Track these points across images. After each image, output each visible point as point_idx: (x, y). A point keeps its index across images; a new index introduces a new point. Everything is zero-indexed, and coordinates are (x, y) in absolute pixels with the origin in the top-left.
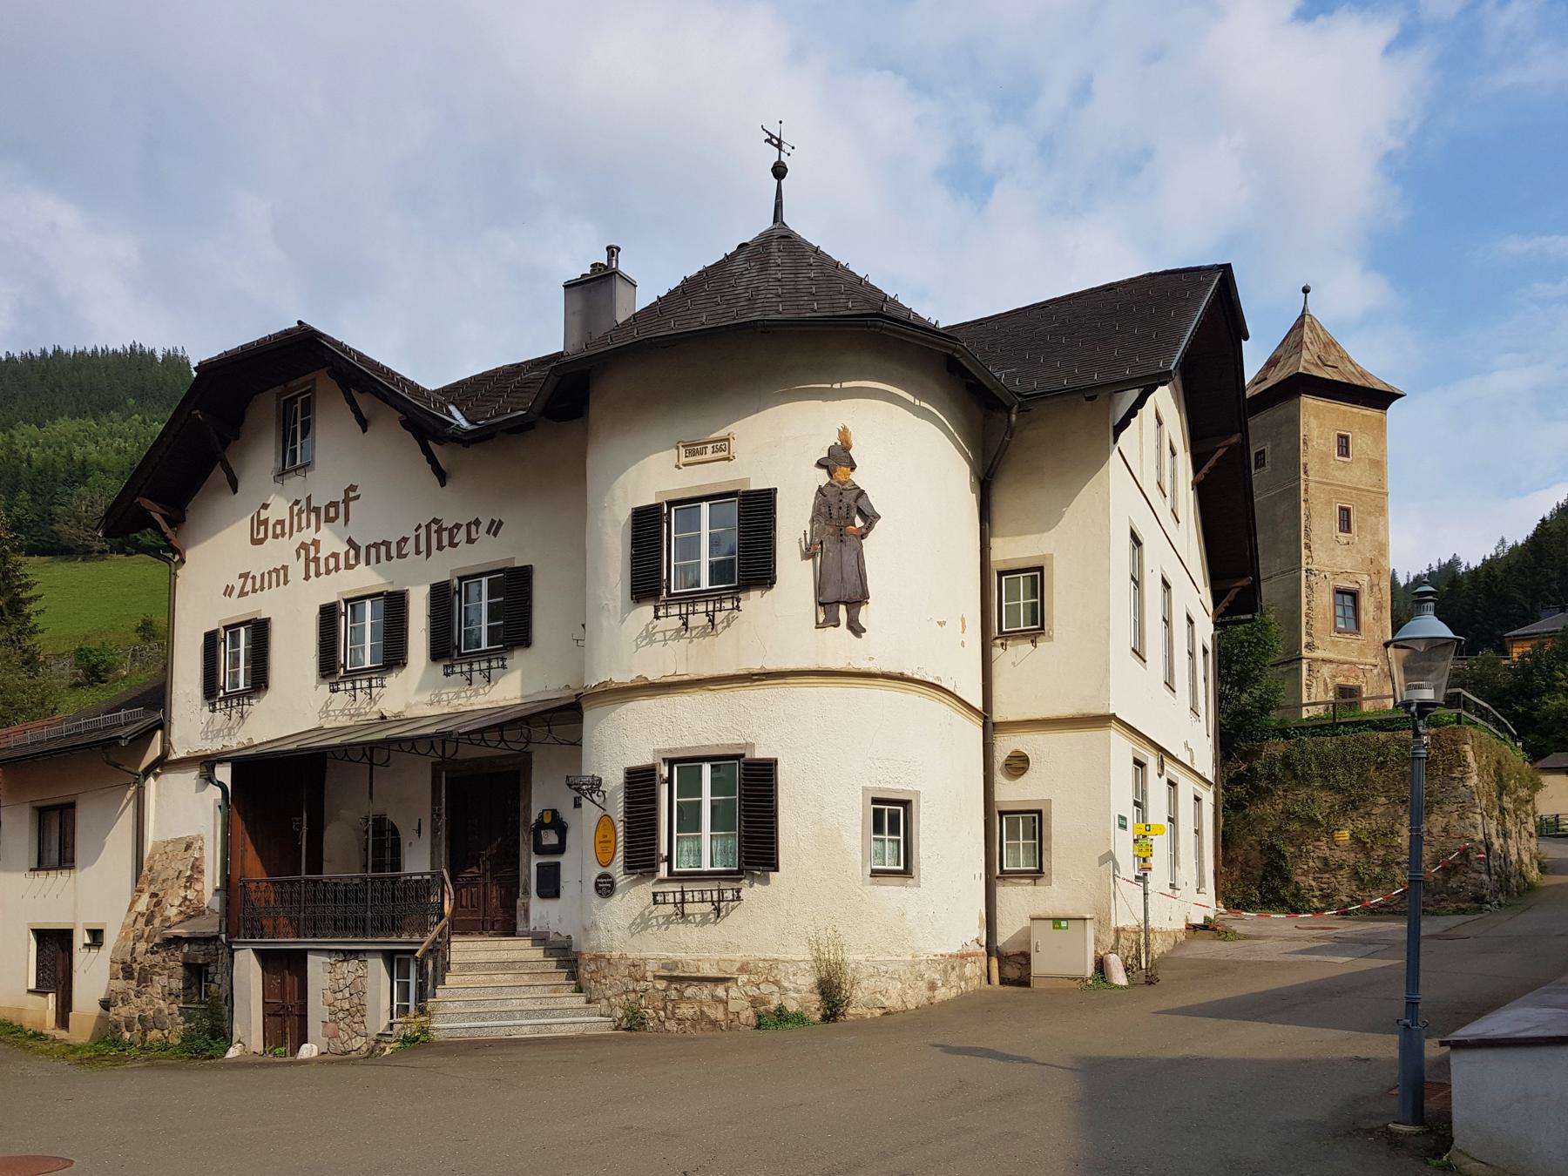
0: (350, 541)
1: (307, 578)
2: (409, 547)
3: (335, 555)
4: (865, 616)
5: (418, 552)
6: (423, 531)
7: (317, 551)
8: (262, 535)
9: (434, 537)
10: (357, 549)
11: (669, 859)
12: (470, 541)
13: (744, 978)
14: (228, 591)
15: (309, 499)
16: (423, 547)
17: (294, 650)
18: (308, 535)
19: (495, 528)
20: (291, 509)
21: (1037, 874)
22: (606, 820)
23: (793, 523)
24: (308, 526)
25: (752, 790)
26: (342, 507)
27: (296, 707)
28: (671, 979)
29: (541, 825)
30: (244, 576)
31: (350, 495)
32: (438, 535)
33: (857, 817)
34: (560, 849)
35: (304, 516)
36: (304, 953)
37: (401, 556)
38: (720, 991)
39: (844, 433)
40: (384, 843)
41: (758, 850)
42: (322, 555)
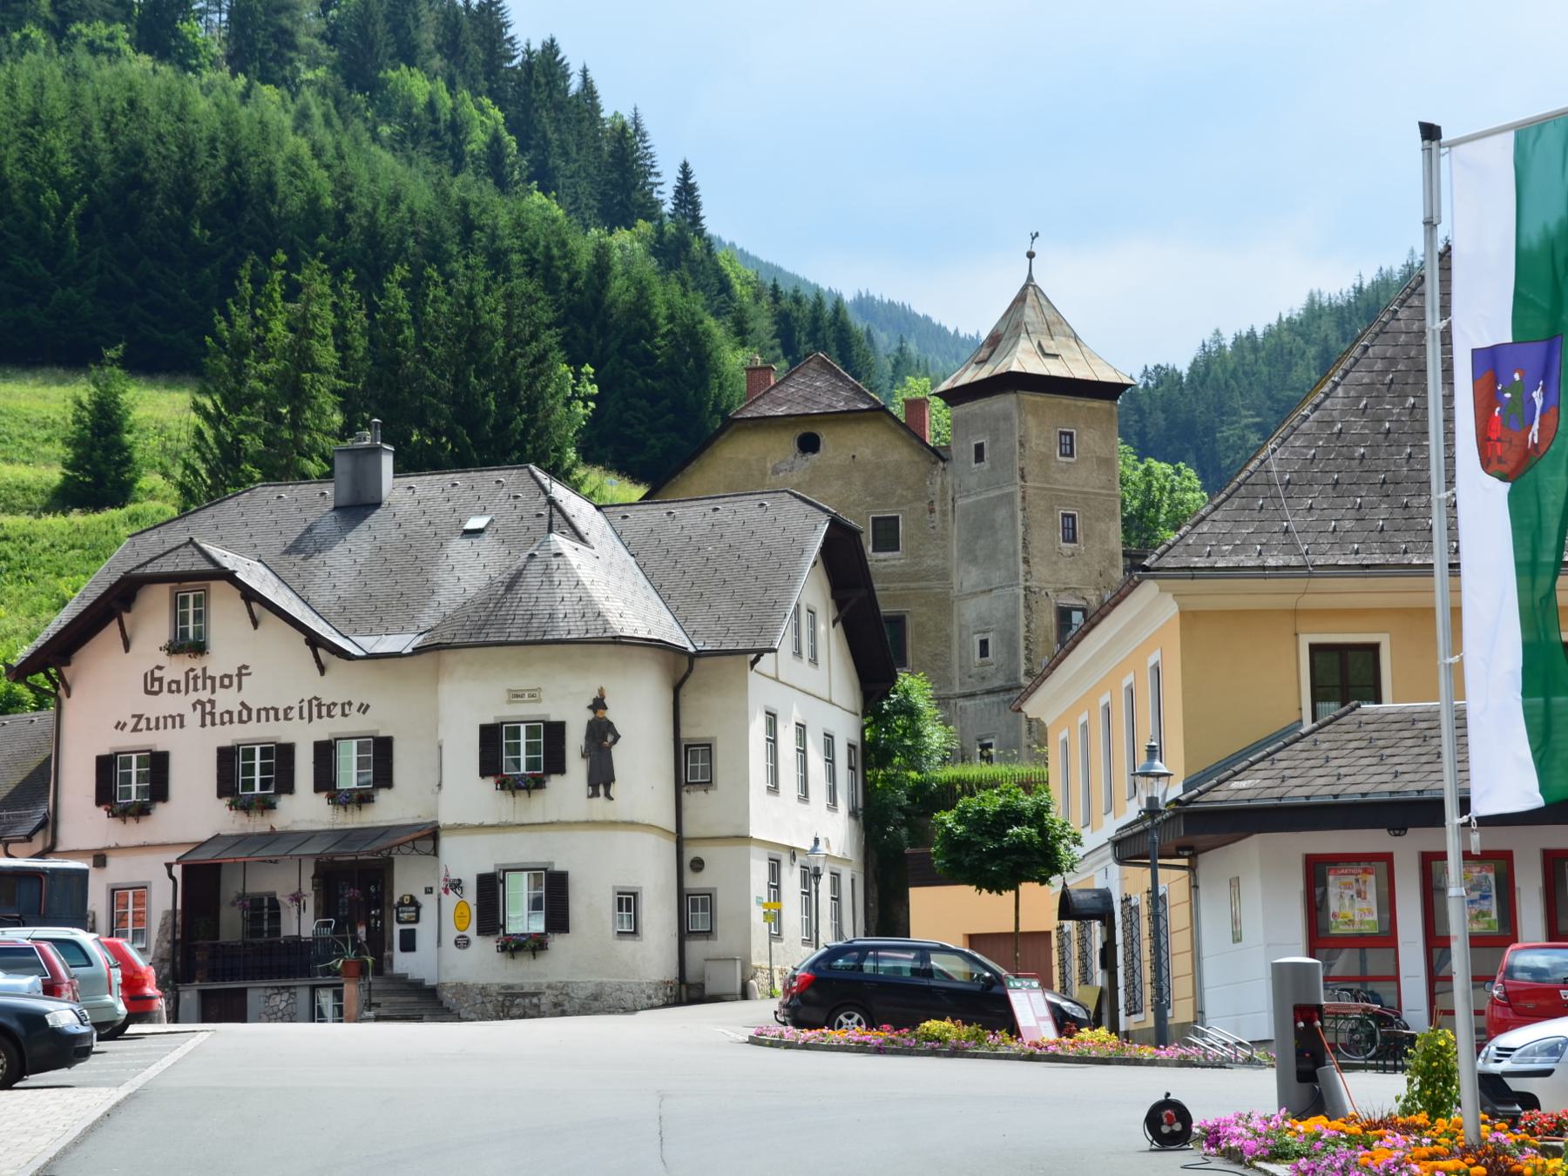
0: (243, 704)
1: (203, 725)
2: (295, 713)
3: (230, 713)
4: (614, 790)
5: (301, 717)
6: (305, 705)
7: (213, 707)
8: (156, 688)
9: (315, 710)
10: (249, 710)
11: (504, 926)
12: (344, 715)
13: (549, 992)
14: (120, 726)
15: (204, 670)
16: (306, 714)
17: (193, 775)
18: (204, 695)
19: (364, 708)
20: (187, 674)
23: (575, 740)
24: (204, 688)
26: (235, 680)
28: (506, 995)
29: (401, 904)
30: (140, 717)
31: (243, 671)
32: (317, 708)
33: (608, 902)
35: (200, 682)
36: (245, 989)
37: (286, 718)
38: (535, 1000)
39: (601, 690)
41: (558, 920)
42: (218, 711)
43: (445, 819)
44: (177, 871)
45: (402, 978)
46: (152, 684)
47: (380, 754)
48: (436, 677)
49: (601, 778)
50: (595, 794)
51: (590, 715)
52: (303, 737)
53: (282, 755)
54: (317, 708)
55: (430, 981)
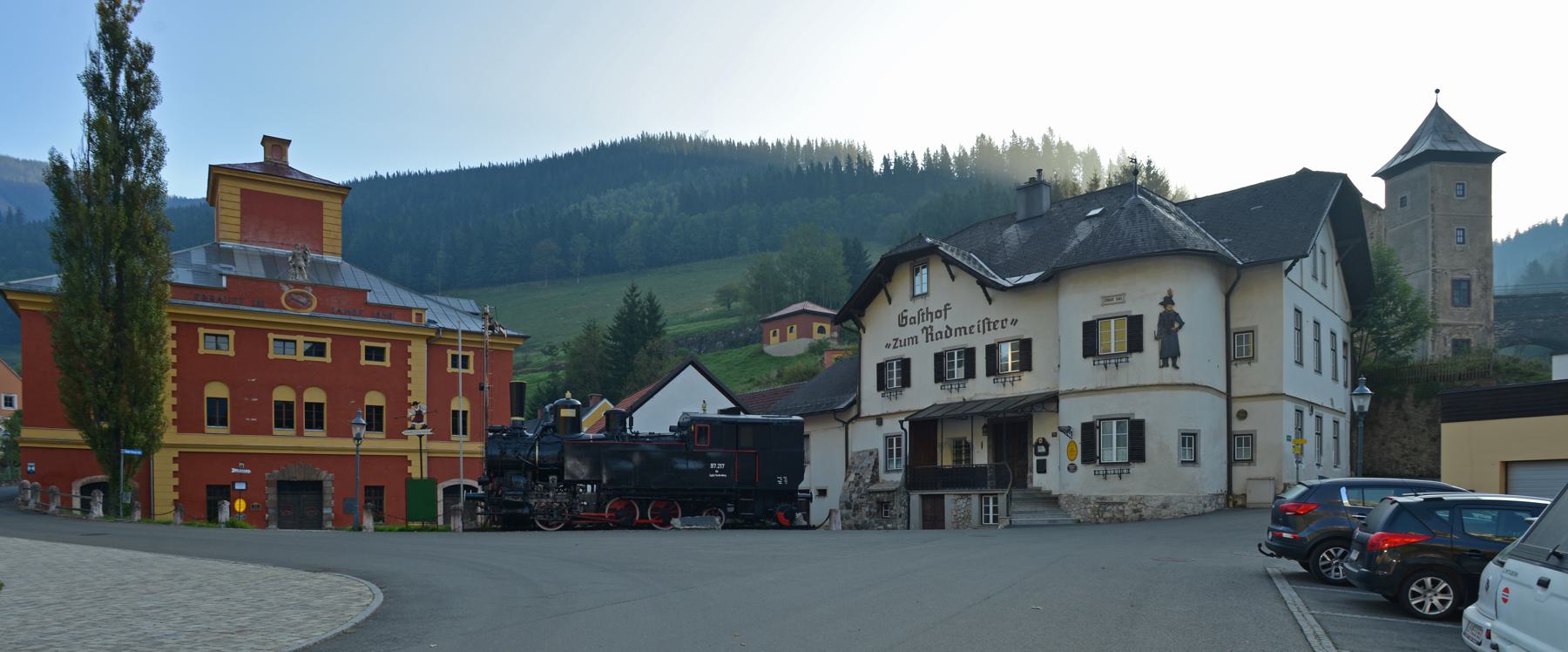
4: (1180, 362)
14: (888, 346)
17: (922, 371)
18: (927, 324)
19: (1014, 322)
21: (1251, 461)
22: (1072, 443)
23: (1150, 327)
25: (1136, 432)
27: (924, 394)
29: (1038, 444)
31: (947, 307)
32: (988, 325)
33: (1174, 442)
34: (1046, 453)
39: (1170, 292)
40: (963, 448)
41: (1137, 453)
43: (1062, 388)
44: (906, 425)
45: (1039, 490)
46: (903, 321)
47: (1024, 349)
48: (1057, 293)
49: (1170, 354)
50: (1165, 365)
51: (1162, 309)
52: (979, 342)
53: (969, 354)
54: (988, 325)
55: (1055, 493)
